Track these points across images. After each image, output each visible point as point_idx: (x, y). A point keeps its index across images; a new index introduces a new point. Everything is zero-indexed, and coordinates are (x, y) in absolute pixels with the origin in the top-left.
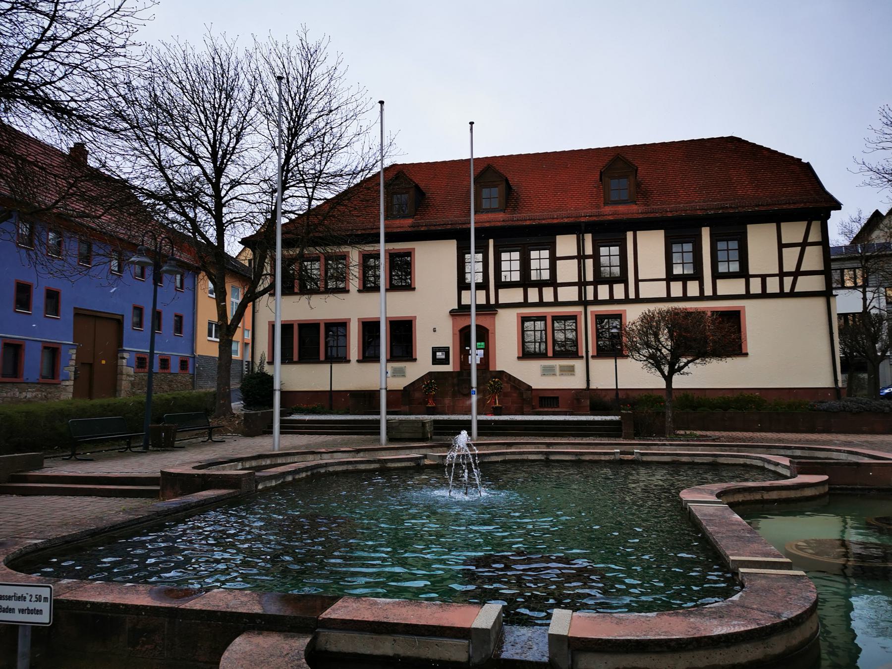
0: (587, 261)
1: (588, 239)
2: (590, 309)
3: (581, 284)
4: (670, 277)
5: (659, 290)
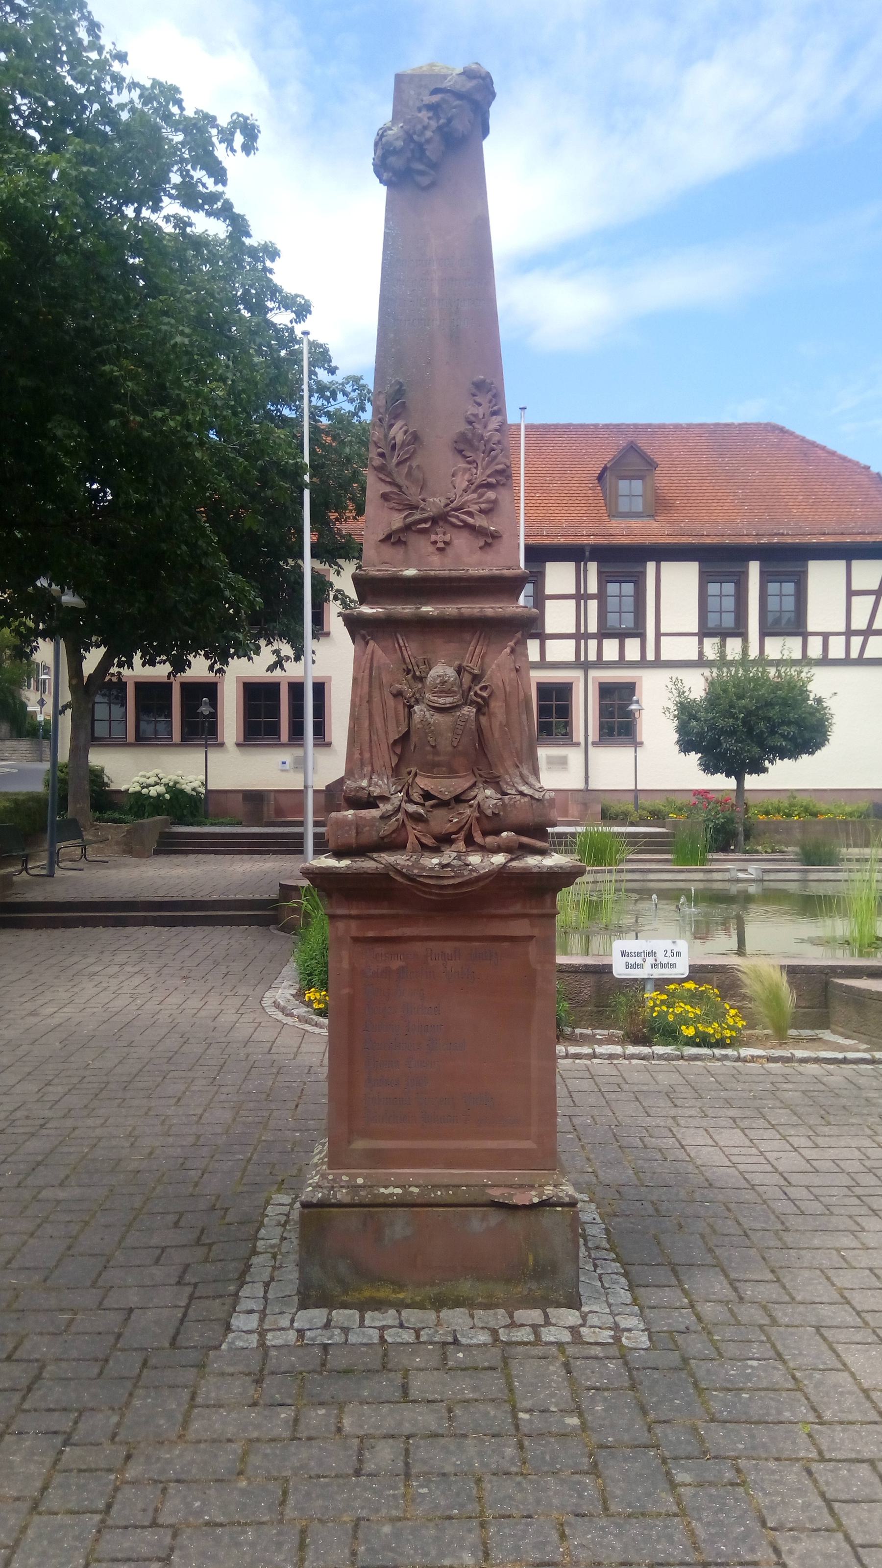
0: (590, 602)
1: (593, 568)
2: (593, 674)
3: (580, 636)
4: (704, 632)
5: (687, 649)
